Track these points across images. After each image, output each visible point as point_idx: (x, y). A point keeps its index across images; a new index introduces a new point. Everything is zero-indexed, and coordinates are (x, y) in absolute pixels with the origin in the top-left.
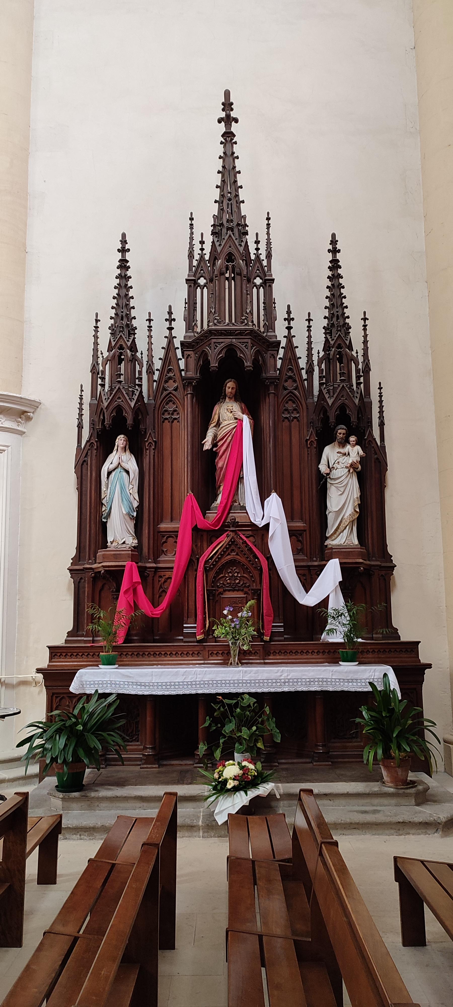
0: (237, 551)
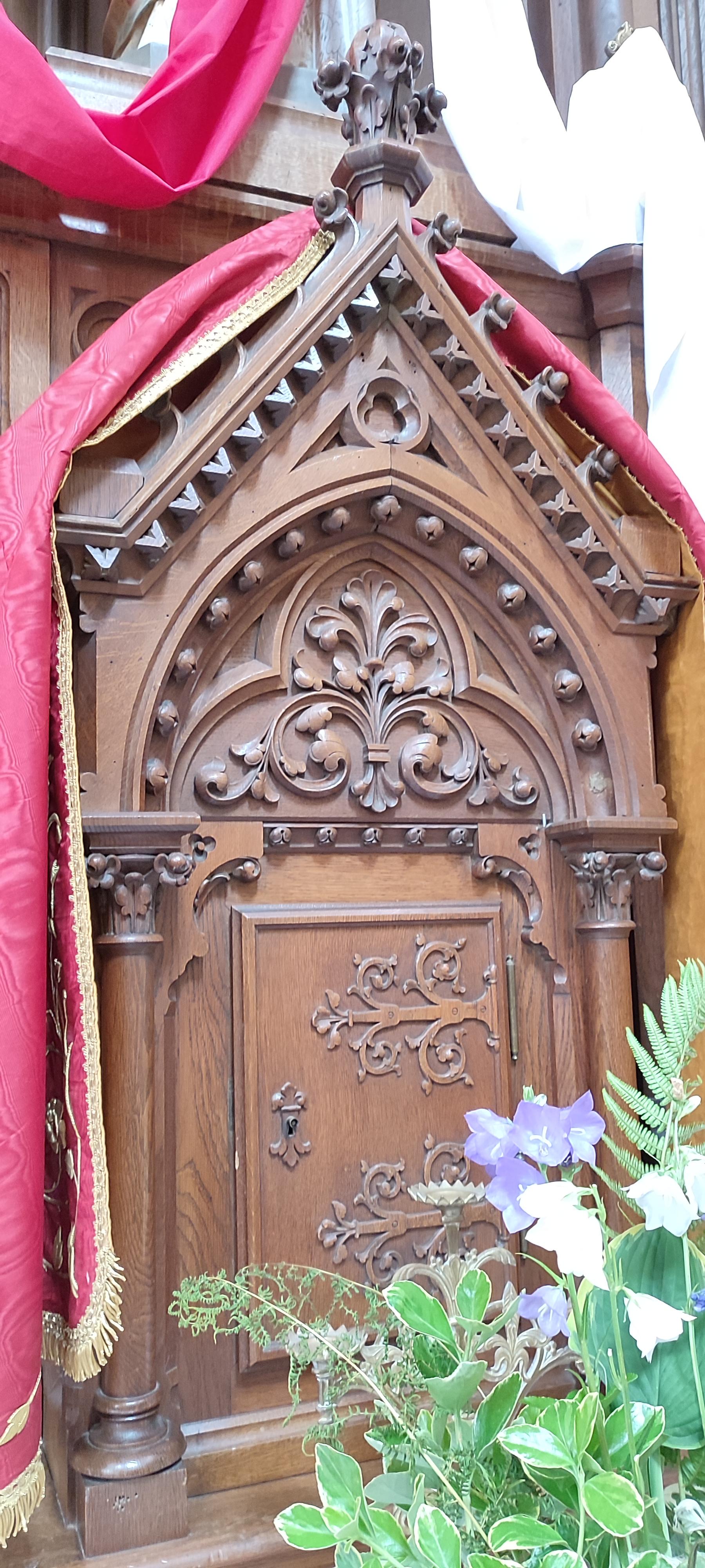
0: (427, 404)
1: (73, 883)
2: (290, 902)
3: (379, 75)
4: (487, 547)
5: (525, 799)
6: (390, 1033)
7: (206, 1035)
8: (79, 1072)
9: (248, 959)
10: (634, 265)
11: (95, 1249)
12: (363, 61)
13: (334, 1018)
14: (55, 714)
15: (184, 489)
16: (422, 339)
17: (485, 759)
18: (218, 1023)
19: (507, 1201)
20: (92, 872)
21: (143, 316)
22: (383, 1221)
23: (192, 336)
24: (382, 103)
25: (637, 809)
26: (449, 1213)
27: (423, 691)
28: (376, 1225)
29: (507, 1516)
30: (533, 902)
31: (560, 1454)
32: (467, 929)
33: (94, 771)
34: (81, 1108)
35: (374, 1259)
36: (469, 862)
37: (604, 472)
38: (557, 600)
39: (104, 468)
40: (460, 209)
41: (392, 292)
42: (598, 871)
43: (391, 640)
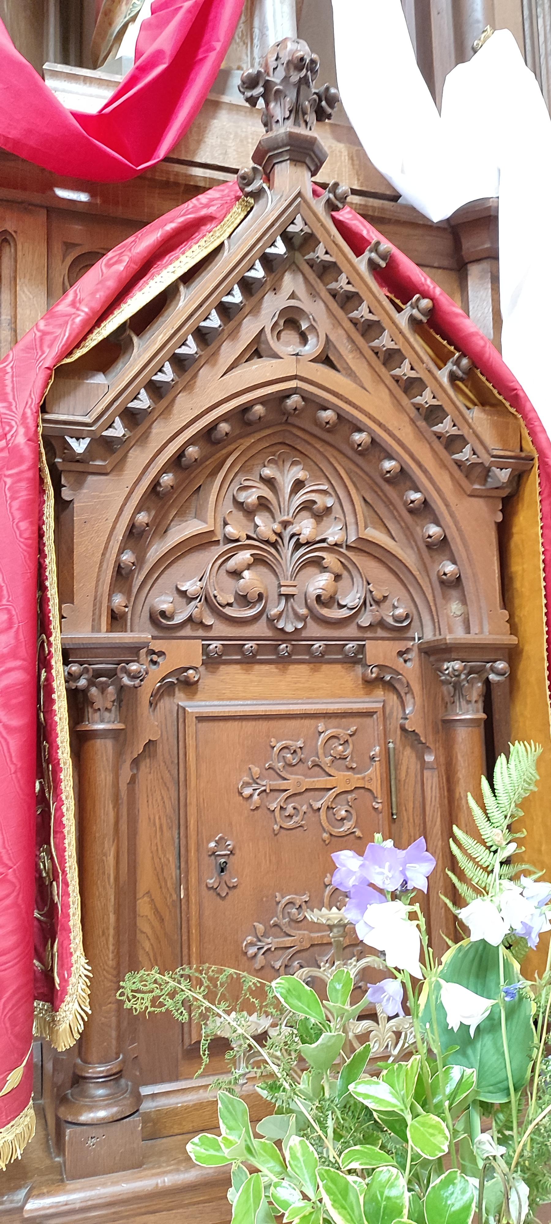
0: (324, 325)
1: (55, 685)
2: (223, 700)
3: (286, 79)
4: (370, 432)
5: (401, 622)
6: (298, 798)
7: (159, 798)
8: (60, 824)
9: (191, 742)
10: (492, 213)
11: (71, 954)
12: (275, 69)
13: (255, 786)
14: (42, 561)
15: (139, 394)
16: (320, 276)
17: (371, 592)
18: (168, 789)
19: (359, 918)
20: (70, 678)
21: (109, 265)
22: (293, 938)
23: (144, 279)
24: (289, 99)
25: (486, 629)
26: (335, 930)
27: (324, 540)
28: (287, 941)
29: (355, 1145)
30: (408, 699)
31: (394, 1101)
32: (358, 720)
33: (72, 603)
34: (61, 850)
35: (286, 966)
36: (359, 669)
37: (460, 373)
38: (425, 471)
39: (79, 379)
40: (358, 175)
41: (297, 242)
42: (456, 676)
43: (298, 502)
